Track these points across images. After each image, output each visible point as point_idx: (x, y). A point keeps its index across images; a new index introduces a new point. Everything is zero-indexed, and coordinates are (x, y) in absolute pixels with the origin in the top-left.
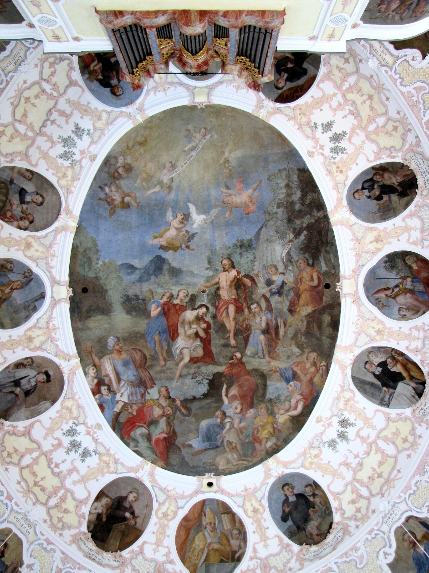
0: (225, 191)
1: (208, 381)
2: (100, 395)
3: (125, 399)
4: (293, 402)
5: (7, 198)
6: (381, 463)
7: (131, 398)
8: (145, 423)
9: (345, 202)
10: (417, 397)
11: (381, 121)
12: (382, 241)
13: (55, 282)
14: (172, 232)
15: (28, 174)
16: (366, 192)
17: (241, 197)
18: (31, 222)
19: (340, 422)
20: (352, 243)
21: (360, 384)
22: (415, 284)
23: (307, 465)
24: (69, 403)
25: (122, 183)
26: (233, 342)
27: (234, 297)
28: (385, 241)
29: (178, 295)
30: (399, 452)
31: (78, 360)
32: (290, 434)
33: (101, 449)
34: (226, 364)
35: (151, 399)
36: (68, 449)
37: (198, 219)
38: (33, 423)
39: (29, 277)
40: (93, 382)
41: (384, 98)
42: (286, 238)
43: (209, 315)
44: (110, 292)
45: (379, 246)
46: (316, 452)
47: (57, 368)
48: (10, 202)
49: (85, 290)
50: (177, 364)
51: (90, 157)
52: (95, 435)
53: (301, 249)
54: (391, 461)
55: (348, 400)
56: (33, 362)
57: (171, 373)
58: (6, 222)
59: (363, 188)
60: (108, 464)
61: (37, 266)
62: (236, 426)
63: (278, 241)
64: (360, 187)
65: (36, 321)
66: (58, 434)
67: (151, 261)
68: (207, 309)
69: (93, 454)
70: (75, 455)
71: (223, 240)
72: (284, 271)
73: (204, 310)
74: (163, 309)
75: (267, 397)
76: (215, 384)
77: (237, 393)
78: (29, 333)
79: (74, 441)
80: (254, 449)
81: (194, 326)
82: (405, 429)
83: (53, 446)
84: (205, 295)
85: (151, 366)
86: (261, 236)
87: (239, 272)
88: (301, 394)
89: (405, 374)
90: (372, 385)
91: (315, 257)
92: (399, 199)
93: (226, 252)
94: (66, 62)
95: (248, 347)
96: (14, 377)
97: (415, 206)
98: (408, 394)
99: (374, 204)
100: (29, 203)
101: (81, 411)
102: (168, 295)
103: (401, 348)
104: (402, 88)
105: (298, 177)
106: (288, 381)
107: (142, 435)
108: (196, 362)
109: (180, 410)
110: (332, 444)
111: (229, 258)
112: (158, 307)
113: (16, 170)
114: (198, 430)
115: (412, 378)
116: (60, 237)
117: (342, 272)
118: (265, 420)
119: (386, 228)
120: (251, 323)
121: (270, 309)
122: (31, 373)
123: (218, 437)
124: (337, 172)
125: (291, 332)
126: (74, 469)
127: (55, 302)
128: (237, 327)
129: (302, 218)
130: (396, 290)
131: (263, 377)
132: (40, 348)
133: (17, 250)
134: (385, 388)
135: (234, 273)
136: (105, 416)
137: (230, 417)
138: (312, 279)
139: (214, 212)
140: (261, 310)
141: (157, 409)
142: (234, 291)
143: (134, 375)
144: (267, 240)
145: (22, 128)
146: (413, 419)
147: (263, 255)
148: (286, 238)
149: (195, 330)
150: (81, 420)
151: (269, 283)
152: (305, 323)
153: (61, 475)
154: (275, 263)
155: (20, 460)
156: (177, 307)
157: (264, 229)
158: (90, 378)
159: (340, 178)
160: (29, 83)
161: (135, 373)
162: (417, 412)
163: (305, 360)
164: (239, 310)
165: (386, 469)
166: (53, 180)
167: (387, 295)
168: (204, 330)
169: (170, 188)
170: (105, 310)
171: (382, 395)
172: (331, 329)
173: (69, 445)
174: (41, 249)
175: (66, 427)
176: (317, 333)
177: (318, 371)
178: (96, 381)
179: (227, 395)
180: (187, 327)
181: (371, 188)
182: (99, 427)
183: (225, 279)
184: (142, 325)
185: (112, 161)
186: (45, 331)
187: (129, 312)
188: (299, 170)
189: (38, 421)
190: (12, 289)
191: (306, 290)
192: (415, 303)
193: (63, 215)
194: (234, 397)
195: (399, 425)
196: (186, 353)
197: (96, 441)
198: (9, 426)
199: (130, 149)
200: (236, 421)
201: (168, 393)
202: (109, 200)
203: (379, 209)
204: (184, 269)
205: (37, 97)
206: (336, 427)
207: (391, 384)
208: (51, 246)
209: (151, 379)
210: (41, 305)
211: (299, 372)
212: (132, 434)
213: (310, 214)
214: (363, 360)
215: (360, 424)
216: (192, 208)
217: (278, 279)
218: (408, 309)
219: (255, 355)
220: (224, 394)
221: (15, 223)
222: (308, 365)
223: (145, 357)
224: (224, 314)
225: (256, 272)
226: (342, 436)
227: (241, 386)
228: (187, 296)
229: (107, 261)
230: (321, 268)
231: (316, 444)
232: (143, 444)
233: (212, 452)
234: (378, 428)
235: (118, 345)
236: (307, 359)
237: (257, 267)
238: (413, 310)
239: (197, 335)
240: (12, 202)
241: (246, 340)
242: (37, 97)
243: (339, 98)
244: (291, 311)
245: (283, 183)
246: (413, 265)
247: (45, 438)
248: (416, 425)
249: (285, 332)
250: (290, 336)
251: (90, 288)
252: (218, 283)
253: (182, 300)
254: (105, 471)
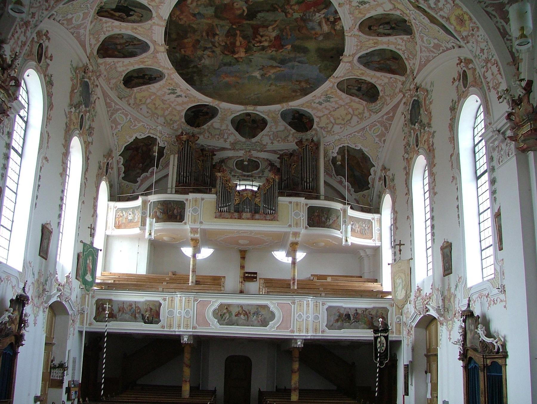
3: (317, 15)
4: (195, 4)
11: (149, 101)
26: (238, 32)
31: (346, 34)
41: (150, 111)
50: (277, 26)
68: (254, 46)
73: (256, 45)
75: (214, 8)
87: (232, 56)
89: (113, 12)
94: (319, 126)
99: (148, 73)
104: (143, 124)
111: (238, 61)
122: (381, 30)
130: (128, 44)
145: (350, 110)
158: (340, 25)
160: (339, 126)
164: (233, 44)
180: (268, 39)
183: (242, 54)
187: (306, 48)
205: (339, 118)
217: (207, 52)
223: (299, 31)
237: (221, 57)
242: (339, 118)
243: (173, 105)
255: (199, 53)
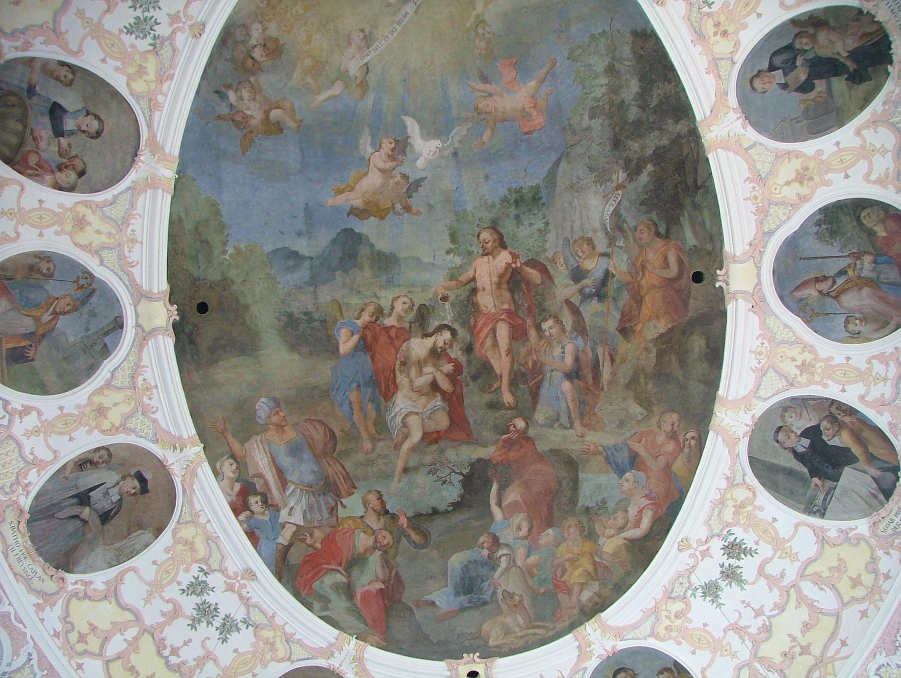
0: (481, 86)
1: (461, 478)
2: (248, 513)
4: (632, 511)
5: (25, 127)
6: (807, 627)
7: (309, 516)
8: (340, 565)
9: (732, 100)
10: (881, 497)
12: (811, 179)
13: (140, 295)
14: (373, 180)
15: (63, 72)
16: (779, 76)
17: (515, 97)
18: (81, 174)
19: (725, 548)
20: (749, 186)
21: (766, 472)
22: (879, 267)
23: (662, 632)
24: (188, 533)
25: (264, 80)
26: (507, 398)
27: (506, 307)
28: (817, 180)
29: (392, 308)
30: (844, 605)
31: (199, 448)
32: (628, 573)
33: (256, 617)
34: (496, 442)
35: (350, 518)
36: (194, 620)
37: (425, 149)
38: (122, 574)
39: (88, 288)
40: (232, 488)
42: (610, 180)
43: (457, 346)
44: (254, 310)
45: (805, 190)
46: (678, 606)
47: (160, 465)
48: (32, 133)
49: (203, 308)
50: (398, 447)
51: (191, 27)
52: (244, 592)
53: (642, 203)
54: (828, 623)
55: (742, 505)
56: (110, 455)
57: (386, 464)
58: (29, 176)
59: (772, 68)
60: (273, 644)
61: (102, 263)
62: (519, 563)
63: (593, 188)
64: (766, 65)
65: (109, 375)
66: (172, 592)
67: (334, 242)
68: (454, 333)
69: (240, 625)
70: (209, 631)
71: (480, 192)
72: (609, 250)
73: (447, 335)
74: (363, 338)
75: (580, 504)
76: (476, 483)
77: (519, 499)
78: (97, 399)
79: (204, 603)
80: (558, 605)
81: (429, 369)
82: (856, 560)
83: (163, 614)
84: (447, 305)
85: (346, 453)
86: (559, 180)
87: (515, 256)
88: (647, 496)
89: (856, 451)
90: (790, 473)
91: (672, 221)
92: (850, 88)
93: (487, 215)
95: (539, 407)
96: (76, 487)
97: (884, 103)
98: (864, 492)
99: (794, 102)
100: (72, 133)
101: (214, 547)
102: (371, 308)
103: (850, 398)
105: (632, 48)
106: (621, 472)
107: (336, 587)
108: (436, 441)
109: (408, 537)
110: (711, 590)
111: (494, 226)
112: (353, 334)
113: (38, 66)
114: (445, 573)
115: (871, 458)
116: (144, 201)
117: (727, 247)
118: (576, 550)
119: (820, 152)
120: (542, 359)
121: (581, 329)
122: (110, 477)
123: (486, 584)
124: (715, 34)
125: (625, 373)
126: (209, 657)
127: (144, 336)
128: (516, 367)
129: (642, 137)
130: (840, 281)
131: (572, 465)
132: (123, 428)
133: (58, 234)
134: (815, 480)
135: (504, 257)
136: (260, 555)
137: (507, 545)
138: (666, 265)
139: (459, 132)
140: (563, 330)
141: (363, 535)
142: (507, 295)
143: (314, 472)
144: (572, 186)
146: (873, 542)
147: (564, 219)
148: (610, 180)
149: (430, 378)
150: (214, 563)
151: (578, 275)
152: (653, 355)
153: (184, 669)
154: (590, 235)
155: (102, 646)
156: (392, 333)
157: (563, 165)
159: (722, 46)
161: (316, 469)
162: (881, 526)
163: (654, 428)
164: (518, 334)
165: (817, 638)
166: (118, 82)
167: (820, 292)
168: (447, 375)
169: (363, 85)
170: (247, 345)
171: (809, 493)
172: (706, 365)
173: (195, 612)
174: (106, 228)
175: (186, 579)
176: (678, 373)
177: (681, 450)
178: (237, 487)
179: (499, 504)
180: (413, 372)
181: (789, 67)
182: (250, 574)
183: (487, 270)
184: (323, 372)
185: (239, 35)
186: (129, 393)
187: (294, 348)
188: (635, 33)
189: (131, 569)
190: (56, 314)
191: (654, 286)
192: (880, 306)
193: (144, 156)
194: (514, 507)
195: (845, 551)
196: (414, 421)
197: (245, 601)
198: (76, 583)
199: (273, 7)
200: (520, 553)
201: (383, 504)
202: (238, 118)
203: (806, 110)
204: (403, 255)
206: (718, 556)
207: (830, 471)
208: (126, 221)
209: (348, 477)
210: (117, 343)
211: (642, 453)
212: (316, 585)
213: (660, 129)
214: (771, 426)
215: (765, 550)
216: (412, 127)
217: (595, 266)
218: (865, 319)
219: (553, 421)
220: (493, 500)
221: (49, 178)
222: (661, 439)
224: (488, 343)
225: (549, 254)
226: (731, 575)
227: (527, 485)
228: (411, 308)
229: (242, 246)
230: (684, 241)
231: (678, 591)
232: (339, 604)
233: (475, 614)
234: (803, 557)
235: (277, 413)
236: (659, 427)
237: (553, 244)
238: (876, 320)
239: (434, 386)
240: (36, 134)
241: (535, 394)
244: (625, 331)
245: (600, 65)
246: (875, 228)
247: (147, 601)
248: (880, 553)
249: (613, 374)
250: (623, 381)
251: (212, 304)
252: (473, 279)
253: (400, 318)
254: (268, 657)
255: (620, 264)
